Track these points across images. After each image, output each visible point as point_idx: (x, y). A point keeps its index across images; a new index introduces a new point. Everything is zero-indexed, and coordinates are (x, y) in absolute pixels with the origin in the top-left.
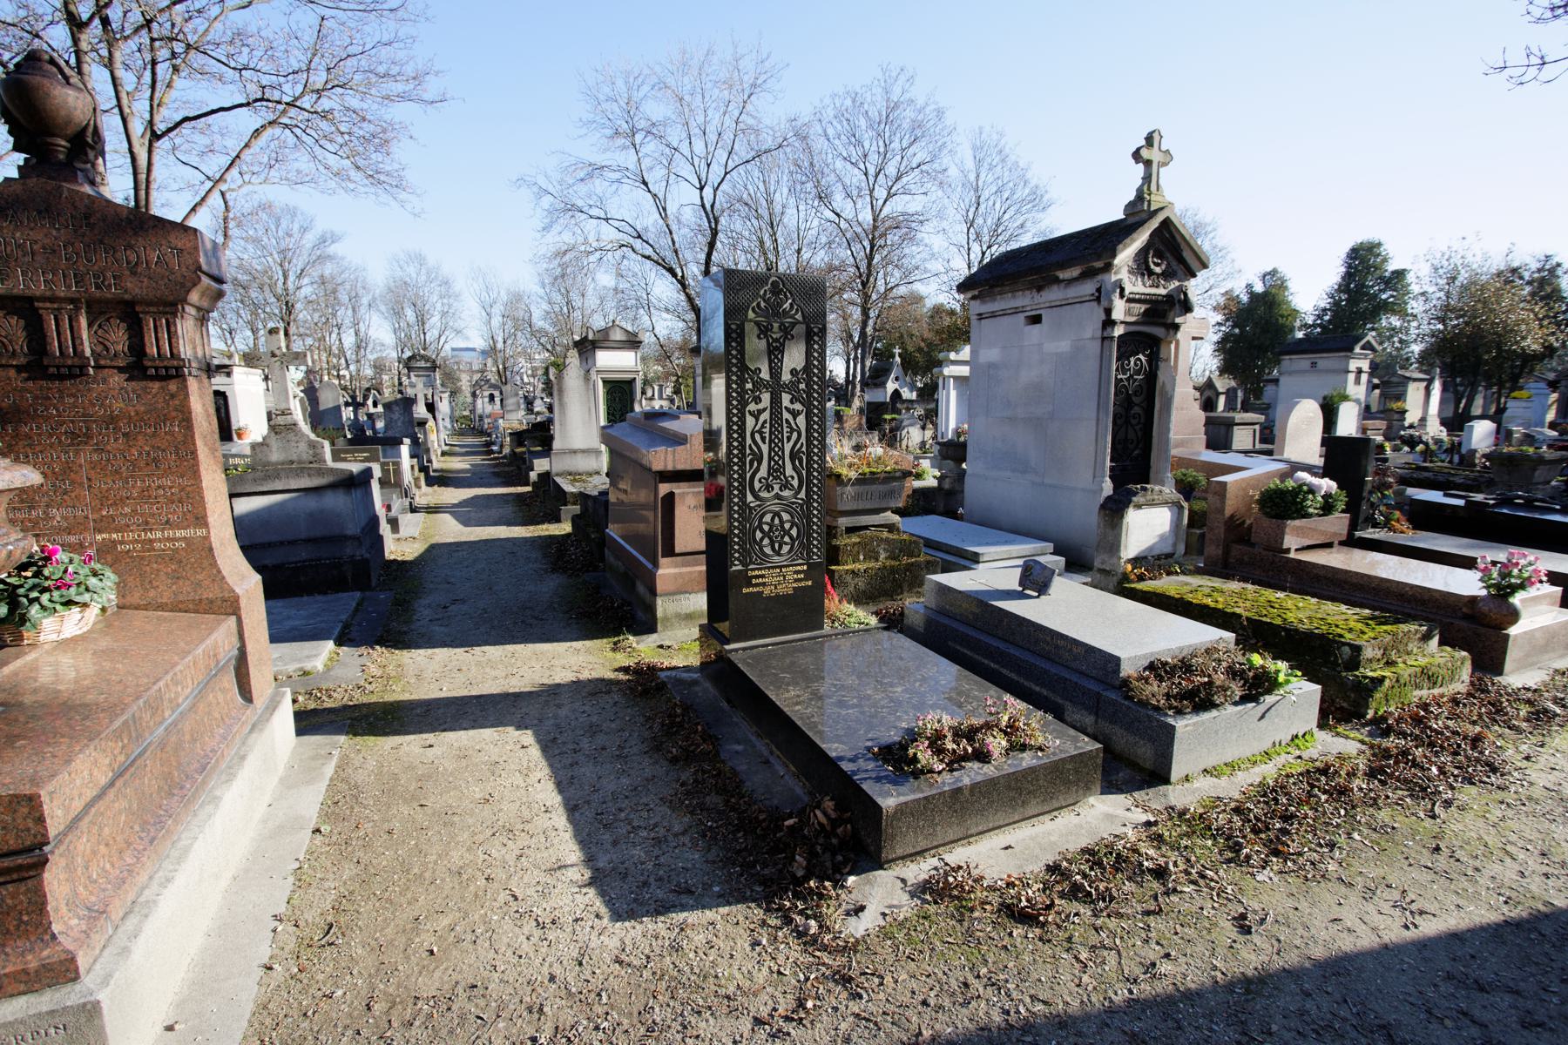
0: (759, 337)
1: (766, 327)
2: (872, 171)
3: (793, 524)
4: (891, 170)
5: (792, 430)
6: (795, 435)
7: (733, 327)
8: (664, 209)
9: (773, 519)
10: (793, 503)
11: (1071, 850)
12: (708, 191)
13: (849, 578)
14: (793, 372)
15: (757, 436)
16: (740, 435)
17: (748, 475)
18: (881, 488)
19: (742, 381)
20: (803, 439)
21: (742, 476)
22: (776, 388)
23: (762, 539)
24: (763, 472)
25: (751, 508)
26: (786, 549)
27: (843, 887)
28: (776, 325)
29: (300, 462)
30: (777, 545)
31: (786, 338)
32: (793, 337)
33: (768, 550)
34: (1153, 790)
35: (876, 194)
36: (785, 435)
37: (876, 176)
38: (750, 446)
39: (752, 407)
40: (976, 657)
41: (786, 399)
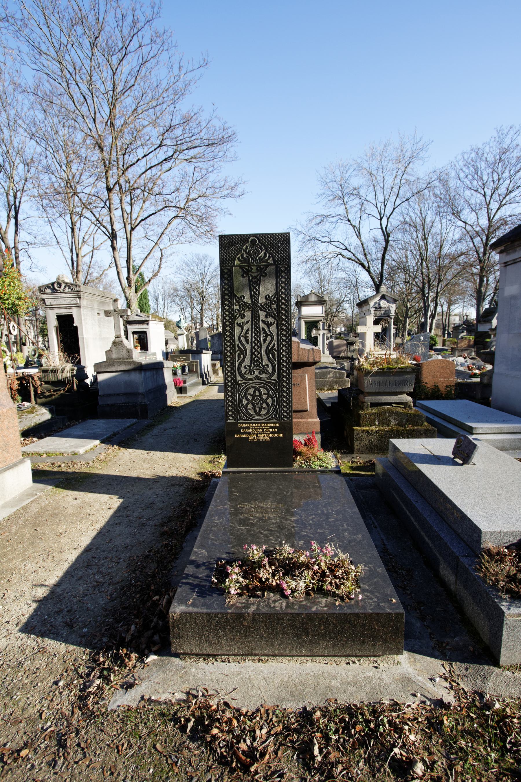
0: (243, 276)
1: (248, 270)
2: (489, 193)
3: (269, 396)
4: (502, 190)
5: (267, 335)
6: (269, 338)
7: (226, 271)
8: (359, 233)
9: (254, 392)
10: (269, 382)
11: (340, 702)
12: (384, 220)
13: (364, 435)
14: (267, 297)
15: (243, 339)
16: (231, 338)
17: (237, 364)
18: (397, 378)
19: (231, 305)
20: (275, 341)
21: (233, 364)
22: (254, 307)
23: (247, 405)
24: (247, 362)
25: (239, 385)
26: (264, 412)
27: (142, 661)
28: (254, 268)
29: (123, 359)
30: (257, 409)
31: (262, 275)
32: (266, 275)
33: (251, 412)
34: (476, 666)
35: (491, 206)
36: (262, 338)
37: (491, 197)
38: (238, 345)
39: (239, 320)
40: (401, 503)
41: (262, 315)
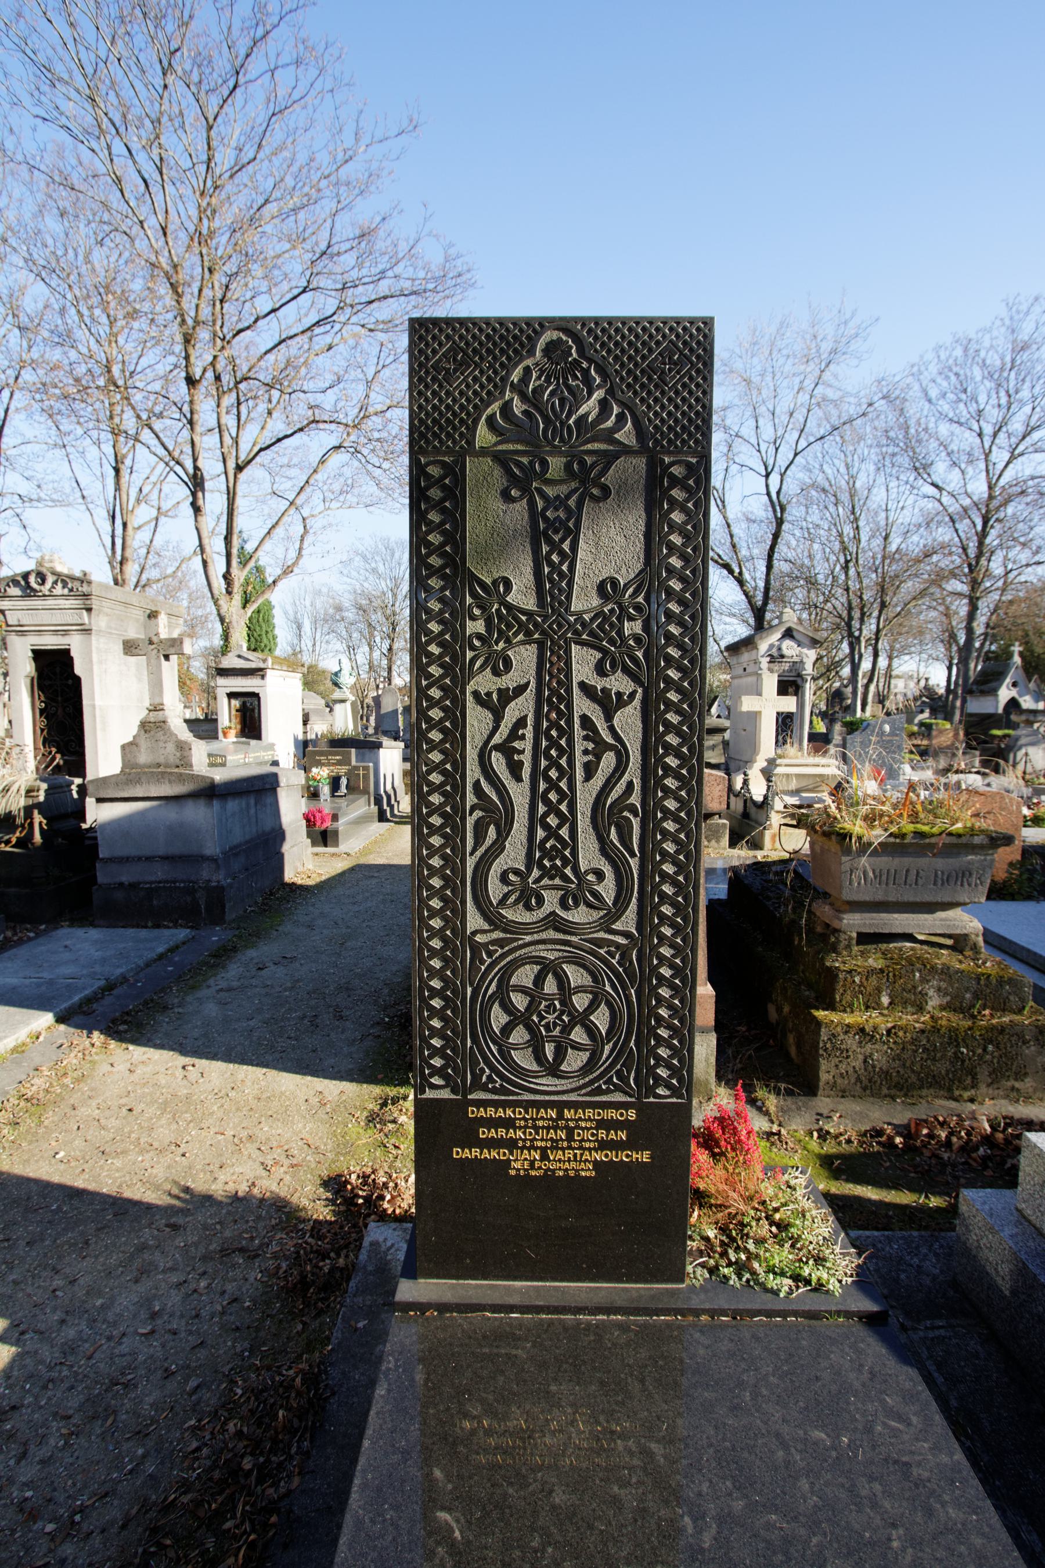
0: (506, 496)
2: (988, 430)
4: (1017, 426)
5: (600, 748)
6: (608, 760)
7: (434, 471)
8: (723, 502)
9: (539, 980)
10: (599, 943)
12: (774, 480)
13: (851, 1042)
14: (607, 589)
15: (498, 762)
17: (471, 863)
18: (941, 864)
20: (633, 773)
23: (507, 1030)
24: (514, 854)
25: (476, 948)
26: (575, 1061)
28: (556, 464)
29: (167, 766)
30: (549, 1049)
32: (606, 491)
33: (524, 1059)
35: (993, 457)
36: (580, 760)
37: (995, 435)
38: (477, 785)
39: (484, 682)
